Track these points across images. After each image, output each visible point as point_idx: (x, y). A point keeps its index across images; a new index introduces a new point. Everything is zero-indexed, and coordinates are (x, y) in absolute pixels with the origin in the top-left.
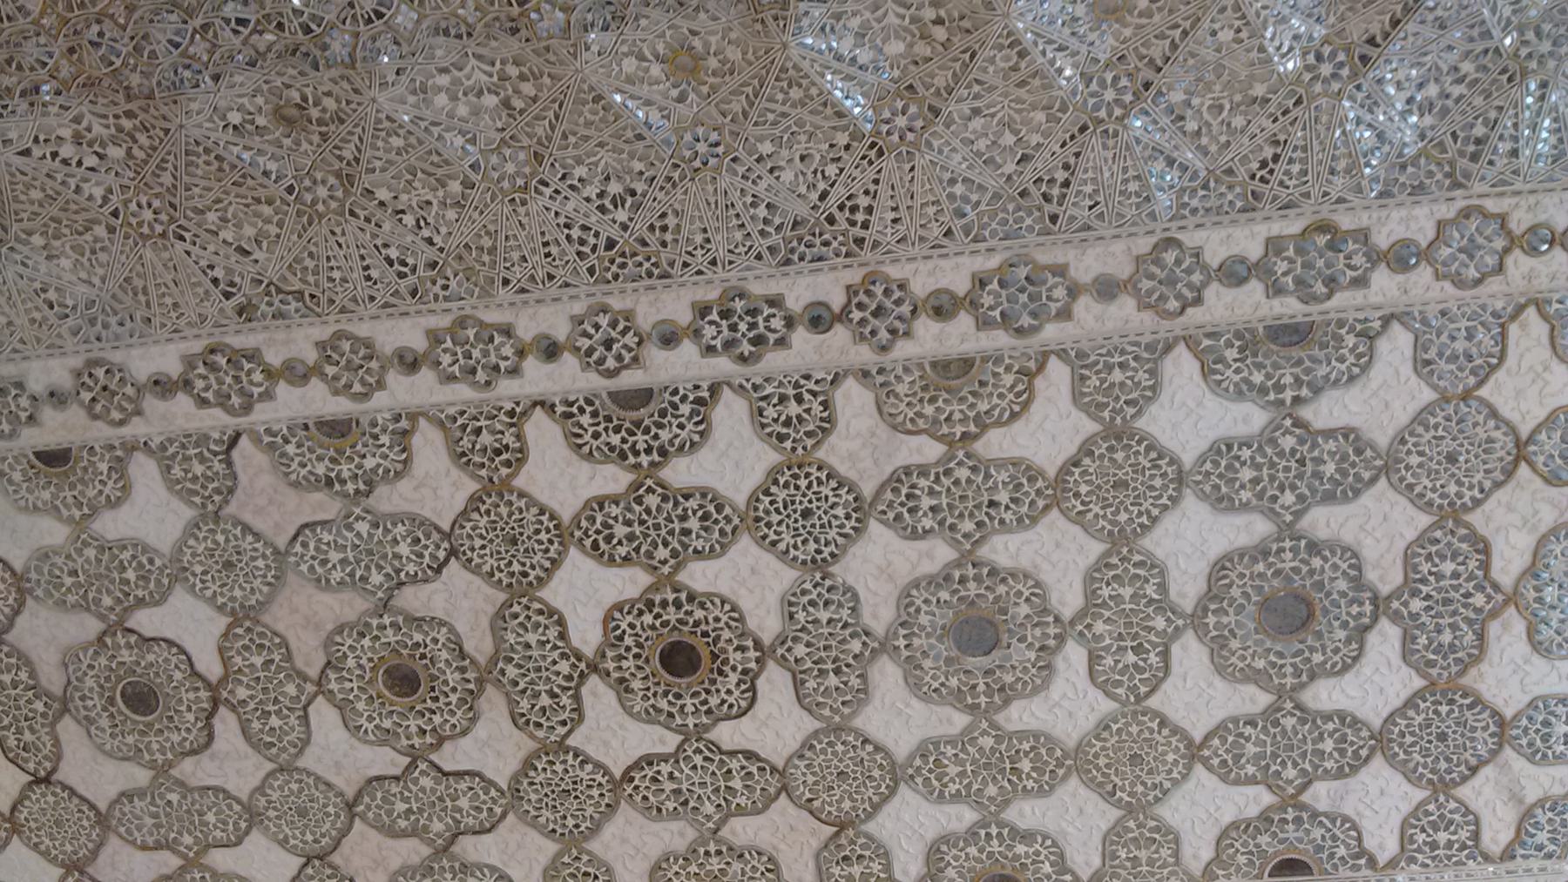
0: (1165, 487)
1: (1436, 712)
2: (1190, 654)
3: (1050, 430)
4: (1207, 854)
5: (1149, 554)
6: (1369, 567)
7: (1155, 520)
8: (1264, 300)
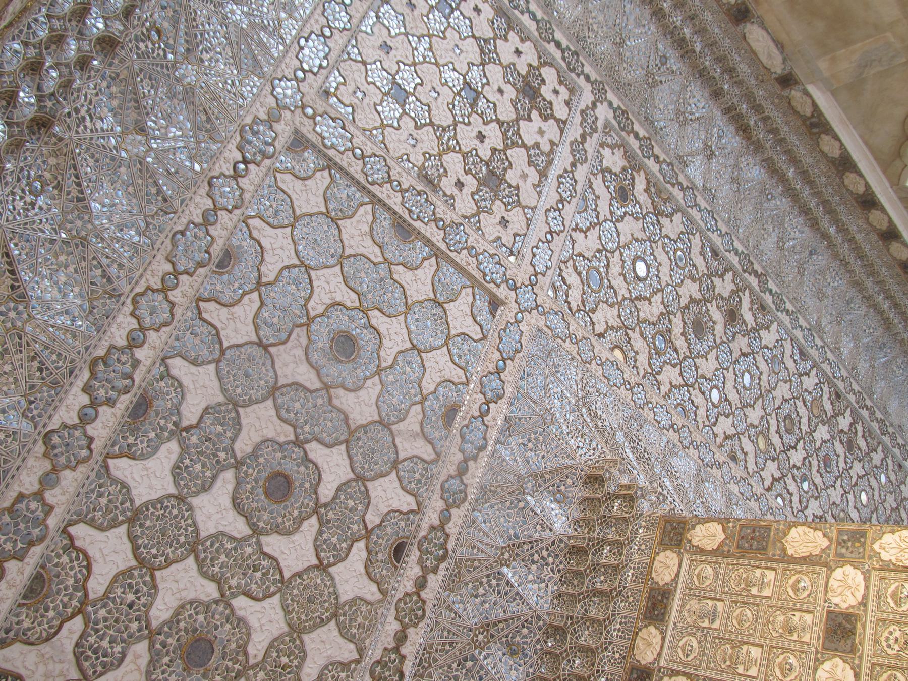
0: (180, 510)
1: (361, 447)
2: (273, 544)
3: (110, 552)
4: (374, 588)
5: (210, 537)
6: (277, 438)
7: (195, 524)
8: (113, 410)
